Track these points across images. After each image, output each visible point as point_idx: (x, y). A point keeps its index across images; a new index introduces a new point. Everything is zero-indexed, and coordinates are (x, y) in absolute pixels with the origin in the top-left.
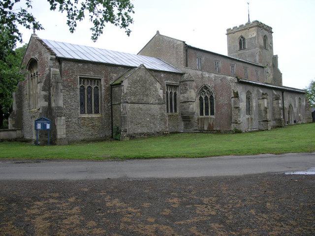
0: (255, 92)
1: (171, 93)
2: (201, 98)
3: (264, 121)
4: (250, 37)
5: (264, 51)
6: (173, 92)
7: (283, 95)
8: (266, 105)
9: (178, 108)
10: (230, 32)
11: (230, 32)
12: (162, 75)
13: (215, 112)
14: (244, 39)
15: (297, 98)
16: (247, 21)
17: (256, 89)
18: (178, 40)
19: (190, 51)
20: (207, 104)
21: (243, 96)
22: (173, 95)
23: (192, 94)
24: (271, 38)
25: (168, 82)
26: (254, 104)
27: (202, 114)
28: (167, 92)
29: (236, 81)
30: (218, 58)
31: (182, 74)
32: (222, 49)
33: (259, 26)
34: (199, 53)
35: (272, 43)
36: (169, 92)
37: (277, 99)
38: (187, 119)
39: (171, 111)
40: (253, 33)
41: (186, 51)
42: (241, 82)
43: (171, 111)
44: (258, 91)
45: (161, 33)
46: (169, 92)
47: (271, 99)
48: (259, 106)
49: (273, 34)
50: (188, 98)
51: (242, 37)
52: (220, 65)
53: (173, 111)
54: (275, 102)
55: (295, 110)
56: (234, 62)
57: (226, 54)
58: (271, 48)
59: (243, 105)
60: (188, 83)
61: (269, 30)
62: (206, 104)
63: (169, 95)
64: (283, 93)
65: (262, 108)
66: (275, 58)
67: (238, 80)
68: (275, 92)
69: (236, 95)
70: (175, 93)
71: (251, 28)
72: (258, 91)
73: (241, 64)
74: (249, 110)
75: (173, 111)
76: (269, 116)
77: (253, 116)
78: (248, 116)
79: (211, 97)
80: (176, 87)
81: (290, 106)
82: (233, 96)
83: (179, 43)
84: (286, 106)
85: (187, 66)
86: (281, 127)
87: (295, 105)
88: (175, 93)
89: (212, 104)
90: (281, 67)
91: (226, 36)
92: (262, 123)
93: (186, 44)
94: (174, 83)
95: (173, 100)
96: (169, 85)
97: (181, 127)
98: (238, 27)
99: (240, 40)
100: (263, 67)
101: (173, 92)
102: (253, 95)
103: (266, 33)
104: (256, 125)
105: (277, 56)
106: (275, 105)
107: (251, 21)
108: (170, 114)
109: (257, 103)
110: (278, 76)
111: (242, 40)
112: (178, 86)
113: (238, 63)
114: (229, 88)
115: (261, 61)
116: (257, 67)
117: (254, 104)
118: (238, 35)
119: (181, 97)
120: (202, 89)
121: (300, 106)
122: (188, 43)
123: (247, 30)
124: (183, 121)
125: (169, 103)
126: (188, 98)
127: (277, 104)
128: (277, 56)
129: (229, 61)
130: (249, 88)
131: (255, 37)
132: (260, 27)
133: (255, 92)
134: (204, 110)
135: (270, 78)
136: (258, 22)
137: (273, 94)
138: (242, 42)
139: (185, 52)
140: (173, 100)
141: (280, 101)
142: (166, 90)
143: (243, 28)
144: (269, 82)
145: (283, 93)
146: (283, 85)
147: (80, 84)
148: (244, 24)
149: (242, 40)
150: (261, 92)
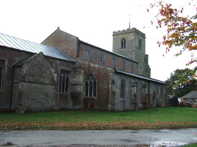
0: (128, 81)
1: (64, 76)
2: (87, 82)
3: (133, 103)
4: (129, 39)
5: (140, 51)
6: (66, 76)
7: (149, 84)
8: (135, 92)
9: (69, 90)
10: (115, 34)
11: (115, 34)
12: (58, 62)
13: (97, 94)
14: (125, 41)
15: (159, 88)
16: (128, 28)
17: (129, 78)
18: (73, 36)
19: (82, 45)
20: (91, 88)
21: (118, 83)
22: (66, 78)
23: (80, 78)
24: (145, 42)
25: (63, 67)
26: (127, 90)
27: (87, 95)
28: (61, 76)
29: (114, 71)
30: (103, 53)
31: (74, 63)
32: (109, 48)
33: (136, 32)
34: (89, 48)
35: (144, 46)
36: (62, 76)
37: (144, 87)
38: (75, 97)
39: (63, 91)
40: (131, 37)
41: (79, 45)
42: (116, 73)
43: (63, 91)
44: (130, 80)
45: (61, 29)
46: (62, 76)
47: (140, 87)
48: (131, 91)
49: (146, 39)
50: (77, 82)
51: (124, 39)
52: (105, 58)
53: (65, 91)
54: (143, 89)
55: (157, 97)
56: (115, 57)
57: (111, 50)
58: (144, 50)
59: (118, 91)
60: (78, 70)
61: (143, 36)
62: (90, 87)
63: (62, 78)
64: (149, 83)
65: (133, 93)
66: (147, 56)
67: (115, 71)
68: (143, 82)
69: (113, 82)
70: (67, 77)
71: (131, 32)
72: (130, 80)
73: (121, 59)
74: (122, 94)
75: (65, 91)
76: (139, 100)
77: (125, 99)
78: (121, 99)
79: (95, 82)
80: (68, 72)
81: (154, 93)
82: (111, 83)
83: (74, 38)
84: (151, 92)
85: (78, 56)
86: (146, 109)
87: (158, 93)
88: (67, 77)
89: (95, 87)
90: (150, 63)
91: (113, 36)
92: (132, 105)
93: (79, 40)
94: (67, 68)
95: (65, 83)
96: (63, 70)
97: (70, 105)
98: (121, 31)
99: (122, 41)
100: (137, 63)
101: (66, 76)
102: (126, 83)
103: (141, 38)
104: (128, 106)
105: (148, 55)
106: (143, 92)
107: (131, 28)
108: (62, 93)
109: (129, 89)
110: (148, 70)
111: (124, 41)
112: (70, 72)
113: (119, 58)
114: (108, 76)
115: (136, 58)
116: (132, 62)
117: (127, 90)
118: (121, 37)
119: (72, 80)
120: (88, 76)
121: (162, 93)
122: (81, 39)
123: (128, 34)
124: (72, 100)
125: (62, 84)
126: (77, 82)
127: (144, 91)
128: (148, 55)
129: (112, 56)
130: (124, 78)
131: (133, 40)
132: (137, 33)
133: (127, 81)
134: (89, 92)
135: (141, 70)
136: (136, 29)
137: (142, 84)
138: (123, 43)
139: (78, 45)
140: (65, 83)
141: (146, 89)
142: (60, 74)
143: (124, 32)
144: (141, 74)
145: (149, 83)
146: (151, 77)
147: (63, 75)
148: (126, 30)
149: (124, 41)
150: (133, 81)
